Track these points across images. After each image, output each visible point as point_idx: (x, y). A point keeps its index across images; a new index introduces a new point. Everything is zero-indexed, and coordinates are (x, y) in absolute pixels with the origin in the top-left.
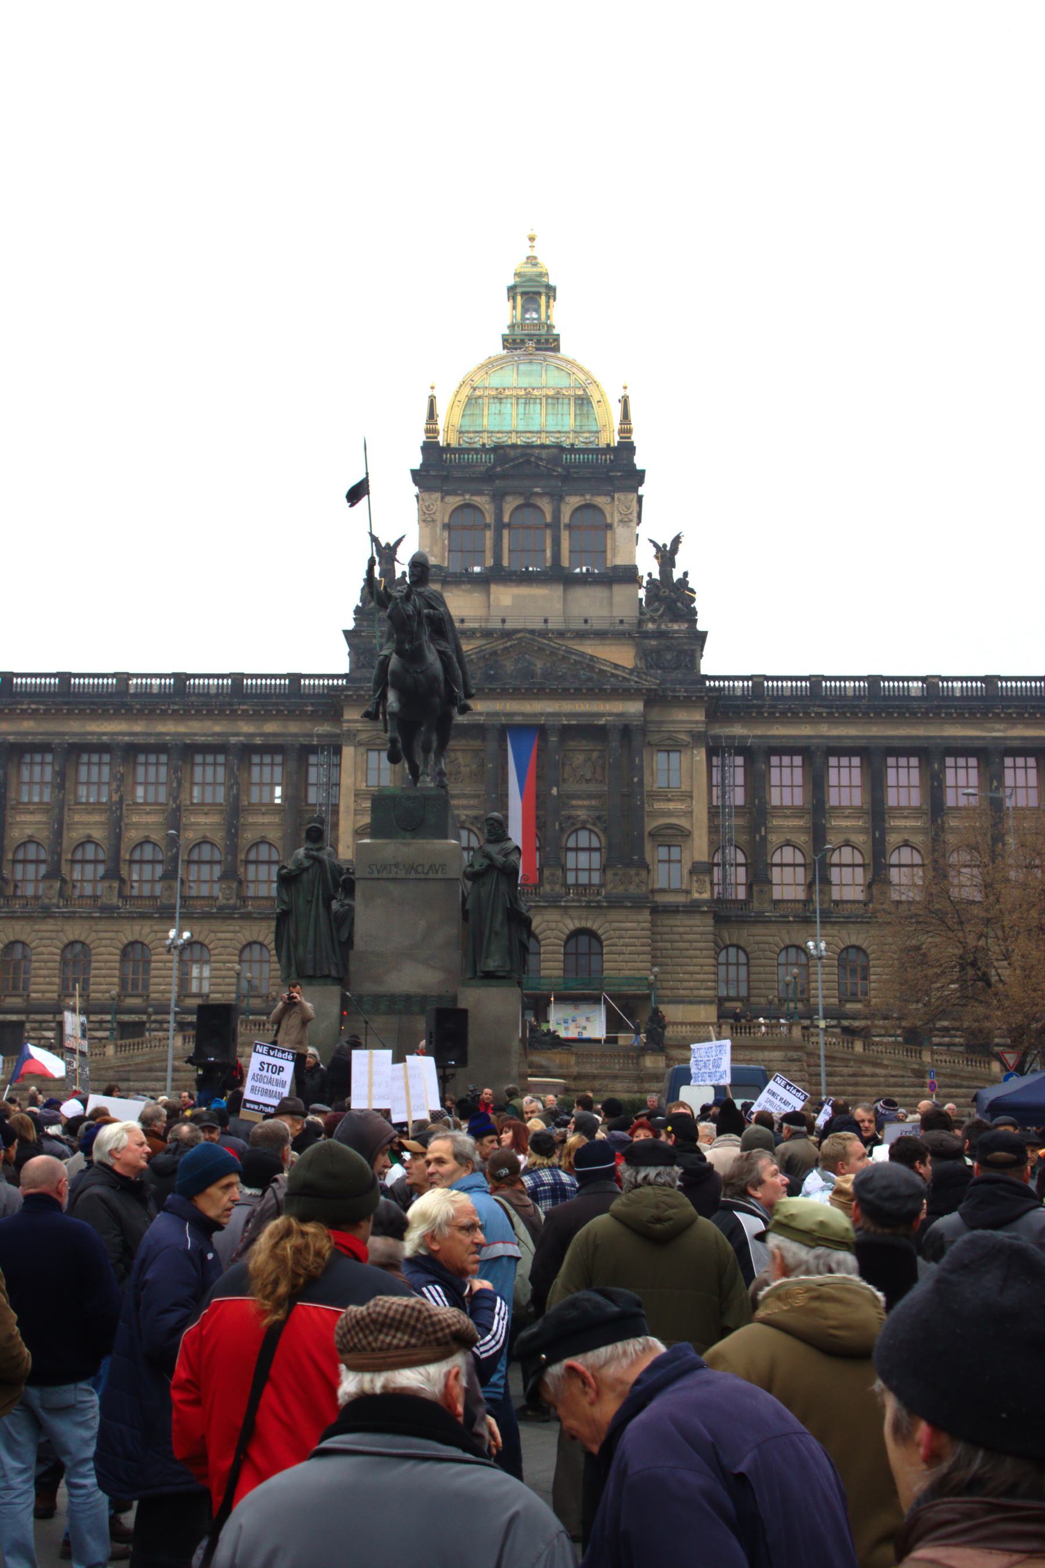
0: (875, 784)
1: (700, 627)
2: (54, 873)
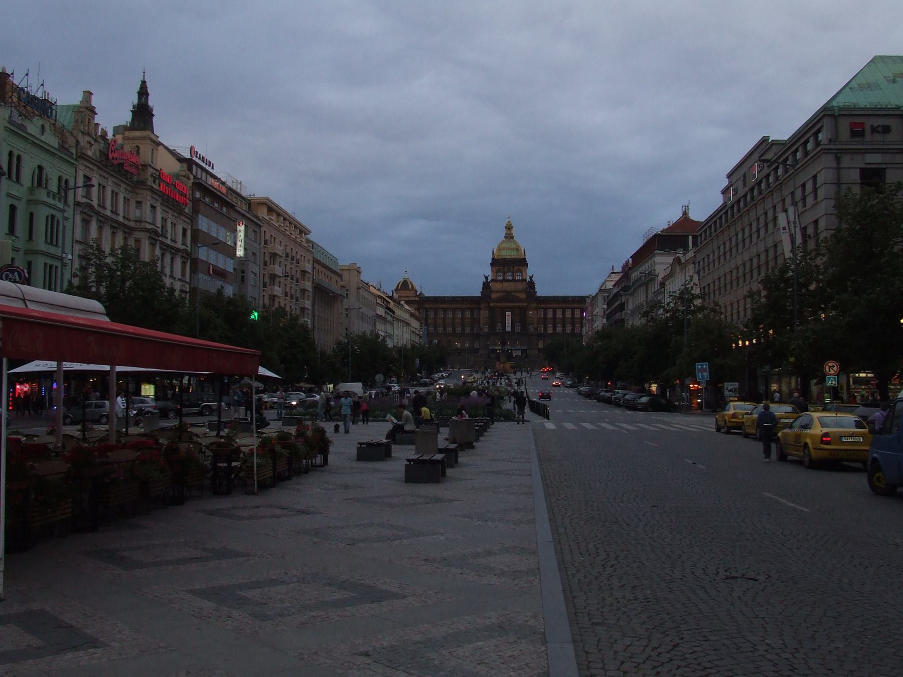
0: (564, 313)
1: (536, 291)
2: (435, 329)
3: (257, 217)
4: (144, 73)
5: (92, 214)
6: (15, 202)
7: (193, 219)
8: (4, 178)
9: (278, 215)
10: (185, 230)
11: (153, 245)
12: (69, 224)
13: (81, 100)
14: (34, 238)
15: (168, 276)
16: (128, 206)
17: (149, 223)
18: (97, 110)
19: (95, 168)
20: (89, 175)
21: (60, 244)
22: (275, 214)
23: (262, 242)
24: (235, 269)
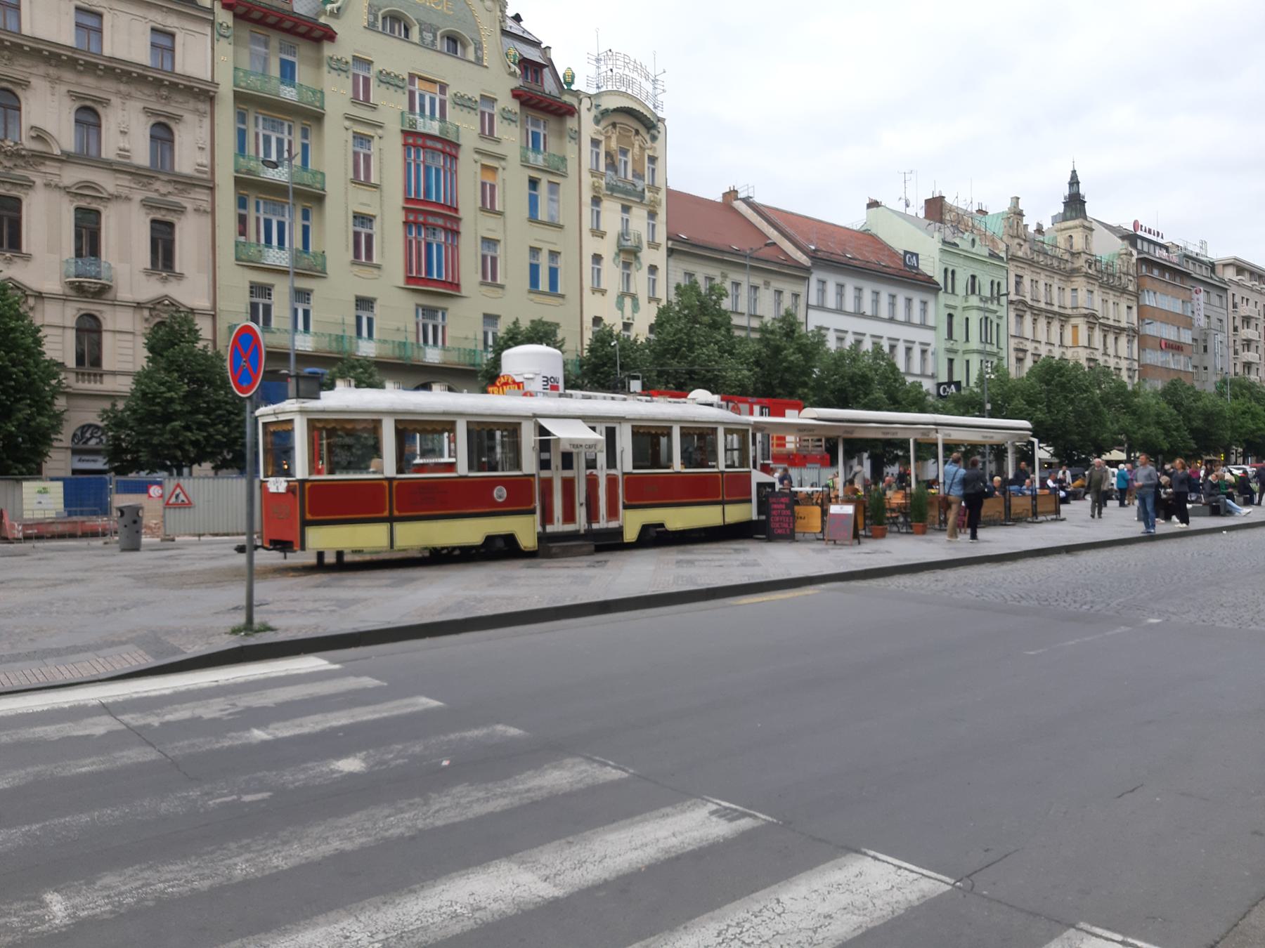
3: (1222, 281)
5: (1025, 309)
6: (952, 311)
7: (1137, 296)
8: (941, 293)
9: (1252, 273)
10: (1129, 308)
11: (1091, 328)
12: (1003, 324)
13: (1009, 206)
14: (970, 339)
15: (1112, 356)
16: (1064, 296)
18: (1024, 213)
19: (1026, 266)
20: (1020, 273)
21: (995, 341)
22: (1247, 275)
23: (1230, 306)
24: (1194, 340)
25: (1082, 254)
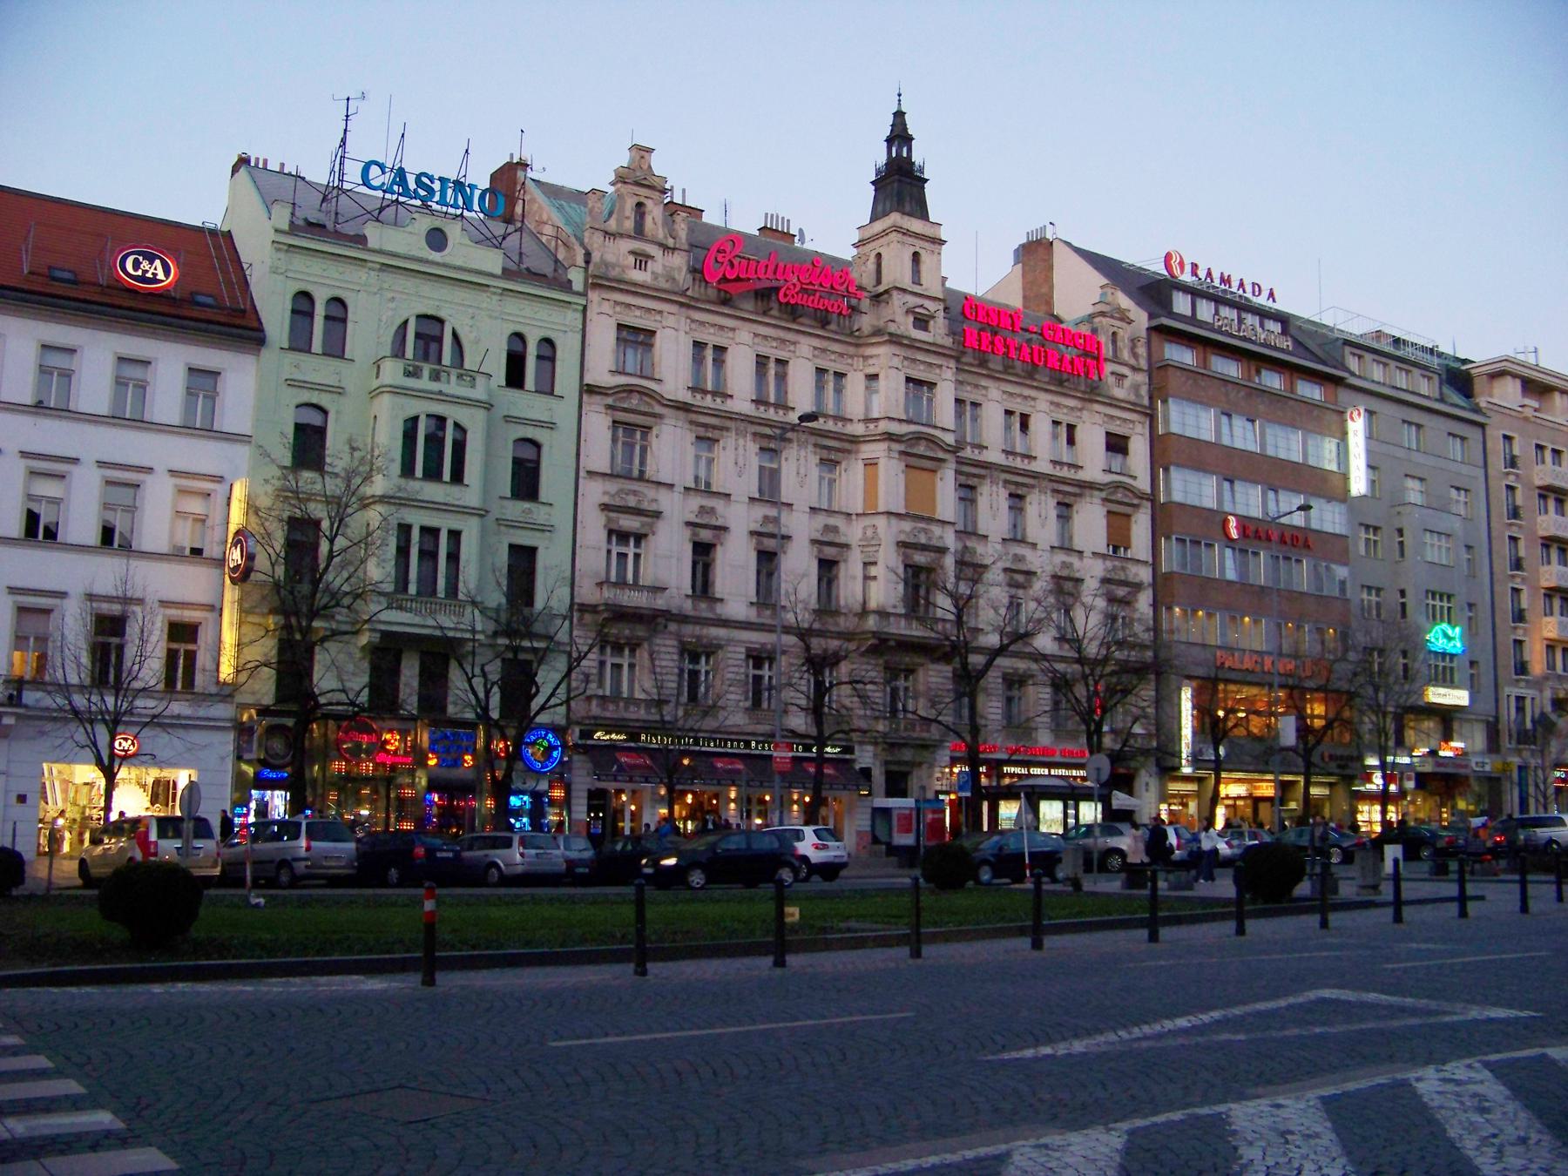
4: (899, 95)
17: (900, 421)
23: (1497, 463)
25: (895, 293)
